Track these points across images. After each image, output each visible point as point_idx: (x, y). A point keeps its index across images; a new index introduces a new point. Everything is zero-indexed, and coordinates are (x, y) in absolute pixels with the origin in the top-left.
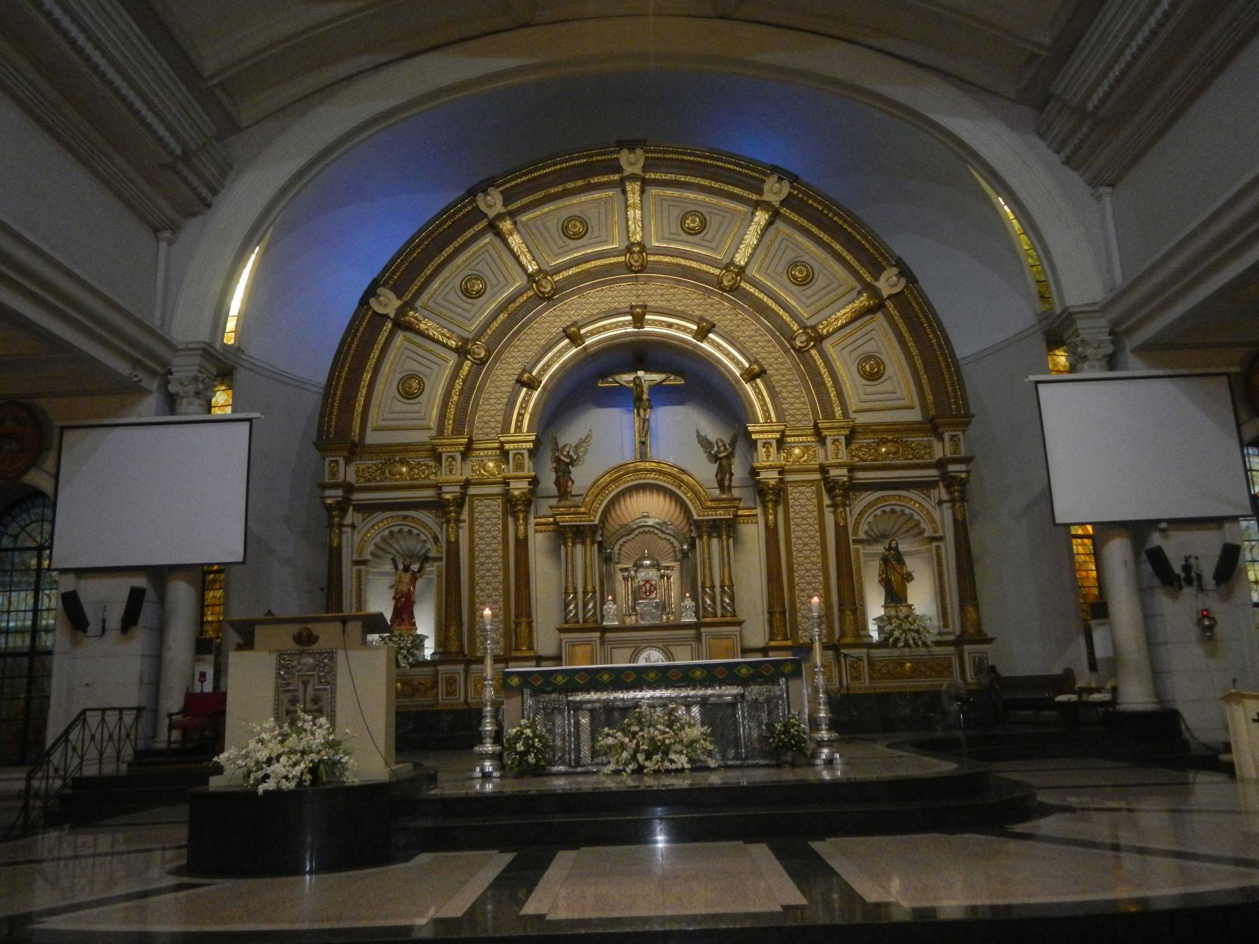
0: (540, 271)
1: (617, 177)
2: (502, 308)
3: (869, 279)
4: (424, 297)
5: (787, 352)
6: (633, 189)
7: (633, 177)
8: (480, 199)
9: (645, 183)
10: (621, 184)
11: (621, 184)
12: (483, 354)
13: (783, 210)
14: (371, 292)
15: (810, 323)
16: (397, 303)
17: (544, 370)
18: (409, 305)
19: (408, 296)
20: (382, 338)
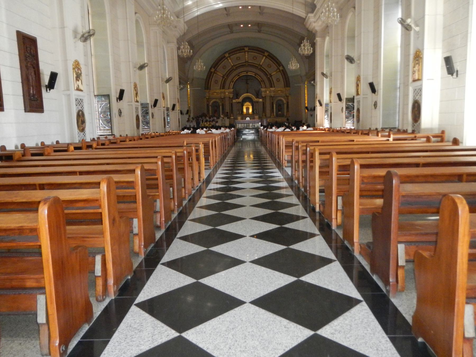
0: (234, 65)
1: (244, 51)
2: (228, 70)
3: (279, 67)
4: (218, 69)
5: (267, 77)
6: (246, 53)
7: (246, 51)
8: (225, 55)
9: (248, 52)
10: (245, 52)
11: (245, 52)
12: (226, 77)
13: (268, 56)
14: (211, 69)
15: (270, 73)
16: (214, 70)
17: (234, 80)
18: (215, 70)
19: (215, 69)
20: (212, 74)
